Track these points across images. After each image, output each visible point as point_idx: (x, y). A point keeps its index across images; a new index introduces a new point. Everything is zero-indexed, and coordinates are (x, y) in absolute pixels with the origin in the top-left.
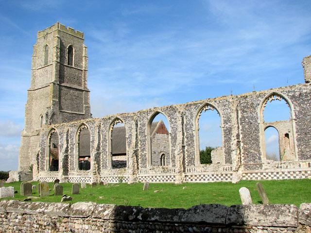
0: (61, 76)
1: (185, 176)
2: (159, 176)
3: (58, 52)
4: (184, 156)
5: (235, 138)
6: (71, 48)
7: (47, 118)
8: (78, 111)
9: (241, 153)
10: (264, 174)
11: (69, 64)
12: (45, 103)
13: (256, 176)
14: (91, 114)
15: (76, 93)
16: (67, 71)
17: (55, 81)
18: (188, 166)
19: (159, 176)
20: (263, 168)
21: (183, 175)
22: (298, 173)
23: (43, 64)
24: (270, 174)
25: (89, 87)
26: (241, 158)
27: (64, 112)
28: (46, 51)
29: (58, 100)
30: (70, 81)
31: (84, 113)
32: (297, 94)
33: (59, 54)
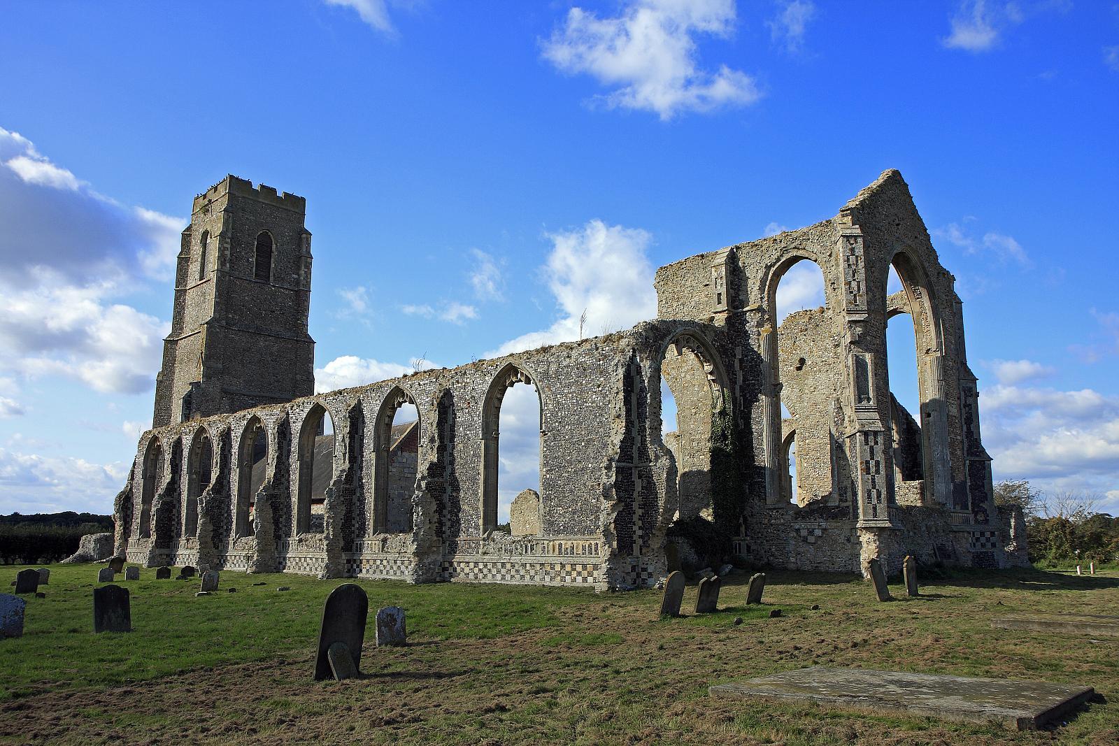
1: (348, 561)
2: (311, 559)
5: (426, 473)
9: (445, 512)
10: (481, 566)
12: (189, 373)
13: (467, 570)
18: (358, 536)
19: (311, 559)
20: (480, 551)
21: (344, 556)
22: (538, 567)
23: (197, 277)
24: (490, 566)
26: (441, 523)
28: (204, 245)
32: (553, 368)
33: (228, 253)
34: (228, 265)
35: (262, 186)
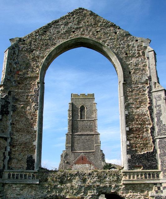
0: (73, 127)
3: (70, 113)
4: (19, 184)
6: (82, 108)
7: (62, 158)
8: (90, 150)
11: (81, 118)
14: (101, 151)
15: (88, 137)
16: (80, 124)
17: (68, 133)
25: (99, 131)
27: (76, 152)
29: (70, 145)
30: (83, 130)
31: (94, 151)
33: (71, 114)
34: (71, 117)
35: (81, 94)
